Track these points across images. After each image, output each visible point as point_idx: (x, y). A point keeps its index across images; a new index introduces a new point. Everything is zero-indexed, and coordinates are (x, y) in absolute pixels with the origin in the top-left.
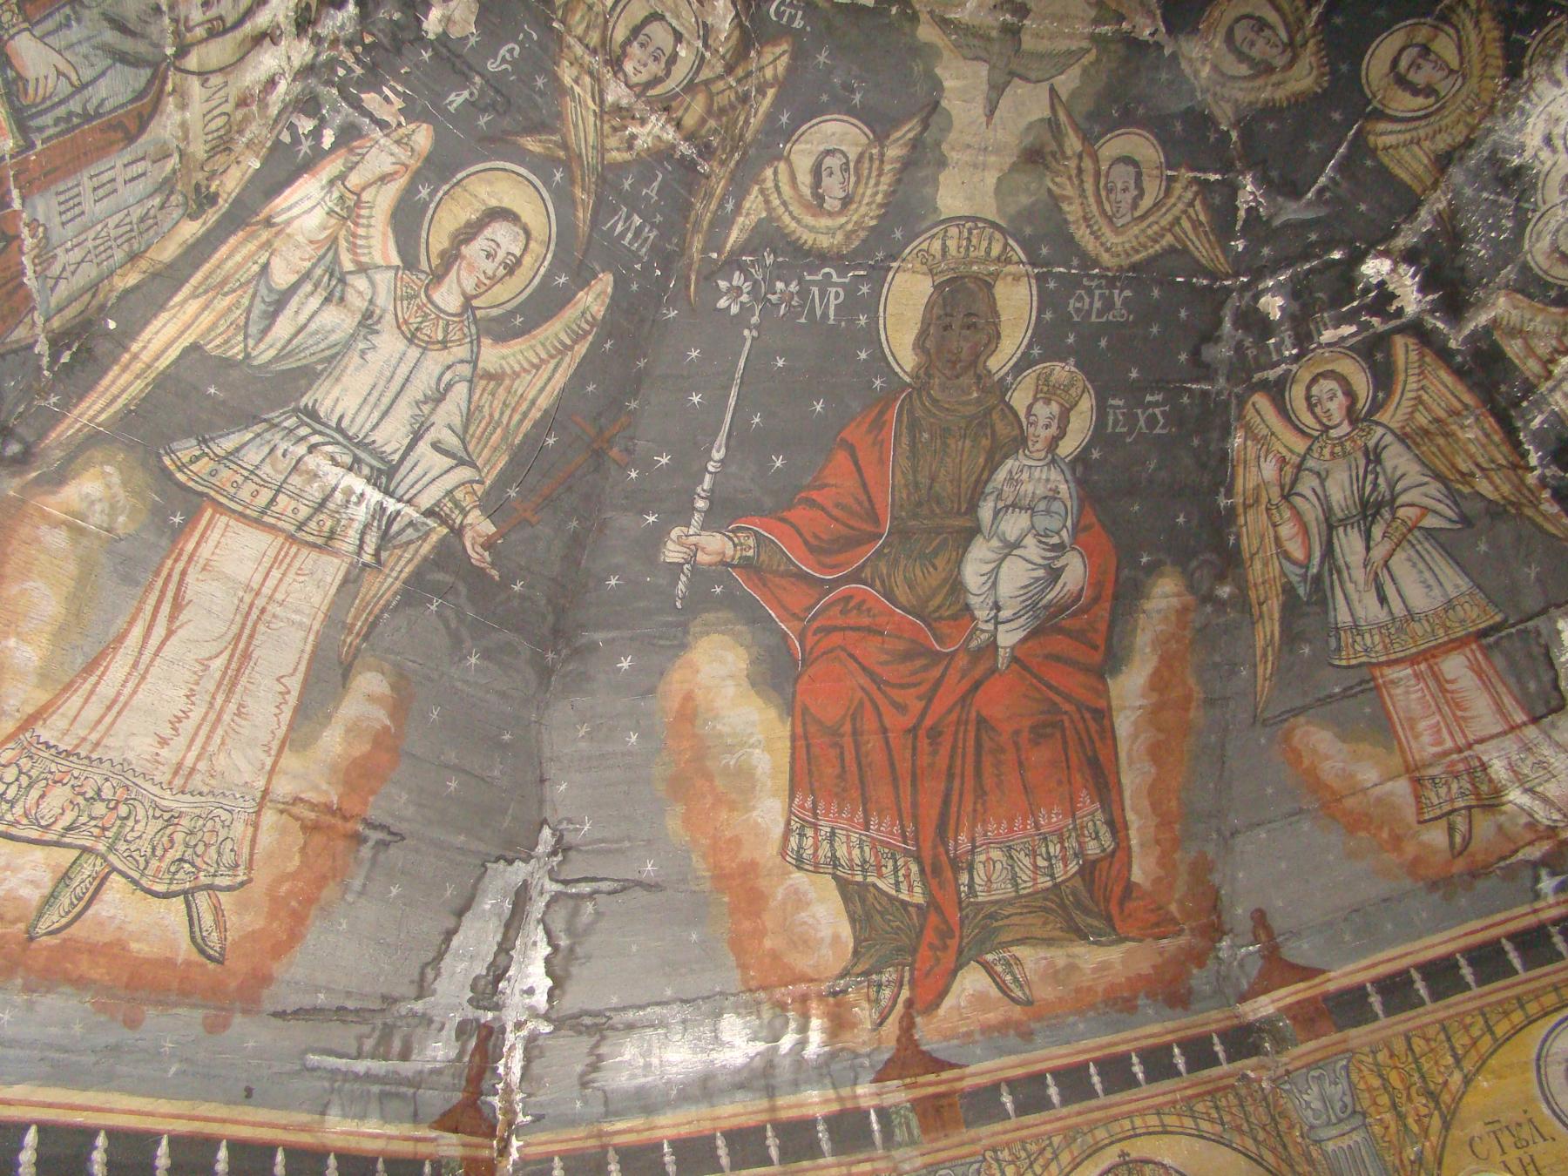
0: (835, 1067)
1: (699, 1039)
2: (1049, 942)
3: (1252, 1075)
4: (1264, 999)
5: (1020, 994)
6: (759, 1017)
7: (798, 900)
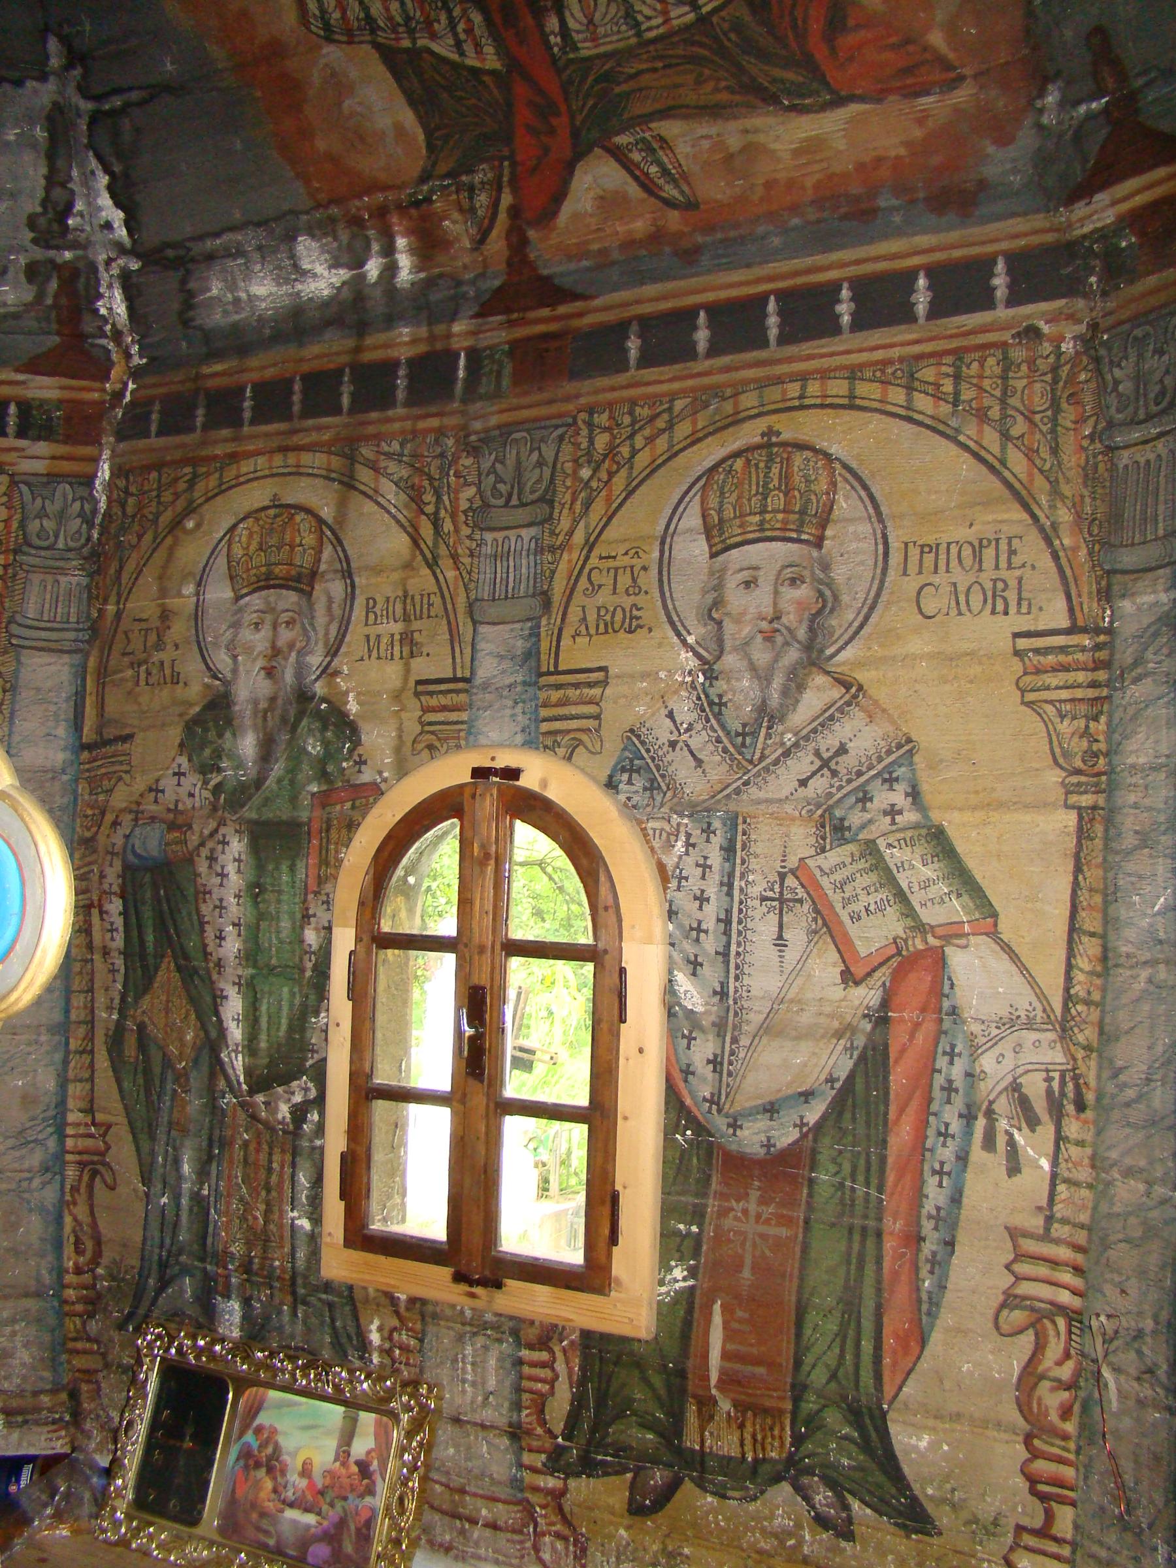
0: (435, 297)
1: (279, 268)
2: (714, 111)
3: (1046, 329)
5: (675, 193)
6: (335, 239)
7: (339, 85)
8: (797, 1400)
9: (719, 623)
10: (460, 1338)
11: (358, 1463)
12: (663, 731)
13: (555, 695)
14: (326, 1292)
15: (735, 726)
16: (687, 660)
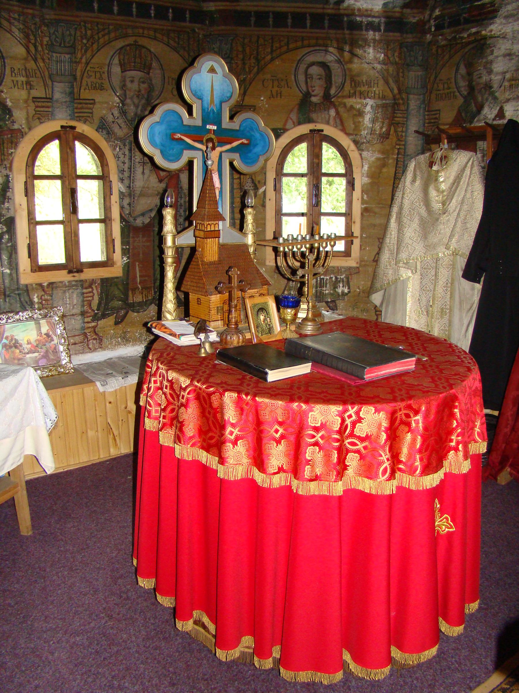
3: (197, 30)
4: (212, 4)
8: (154, 283)
9: (125, 91)
10: (65, 292)
11: (45, 334)
12: (110, 118)
13: (80, 106)
14: (18, 291)
15: (130, 118)
16: (117, 99)
